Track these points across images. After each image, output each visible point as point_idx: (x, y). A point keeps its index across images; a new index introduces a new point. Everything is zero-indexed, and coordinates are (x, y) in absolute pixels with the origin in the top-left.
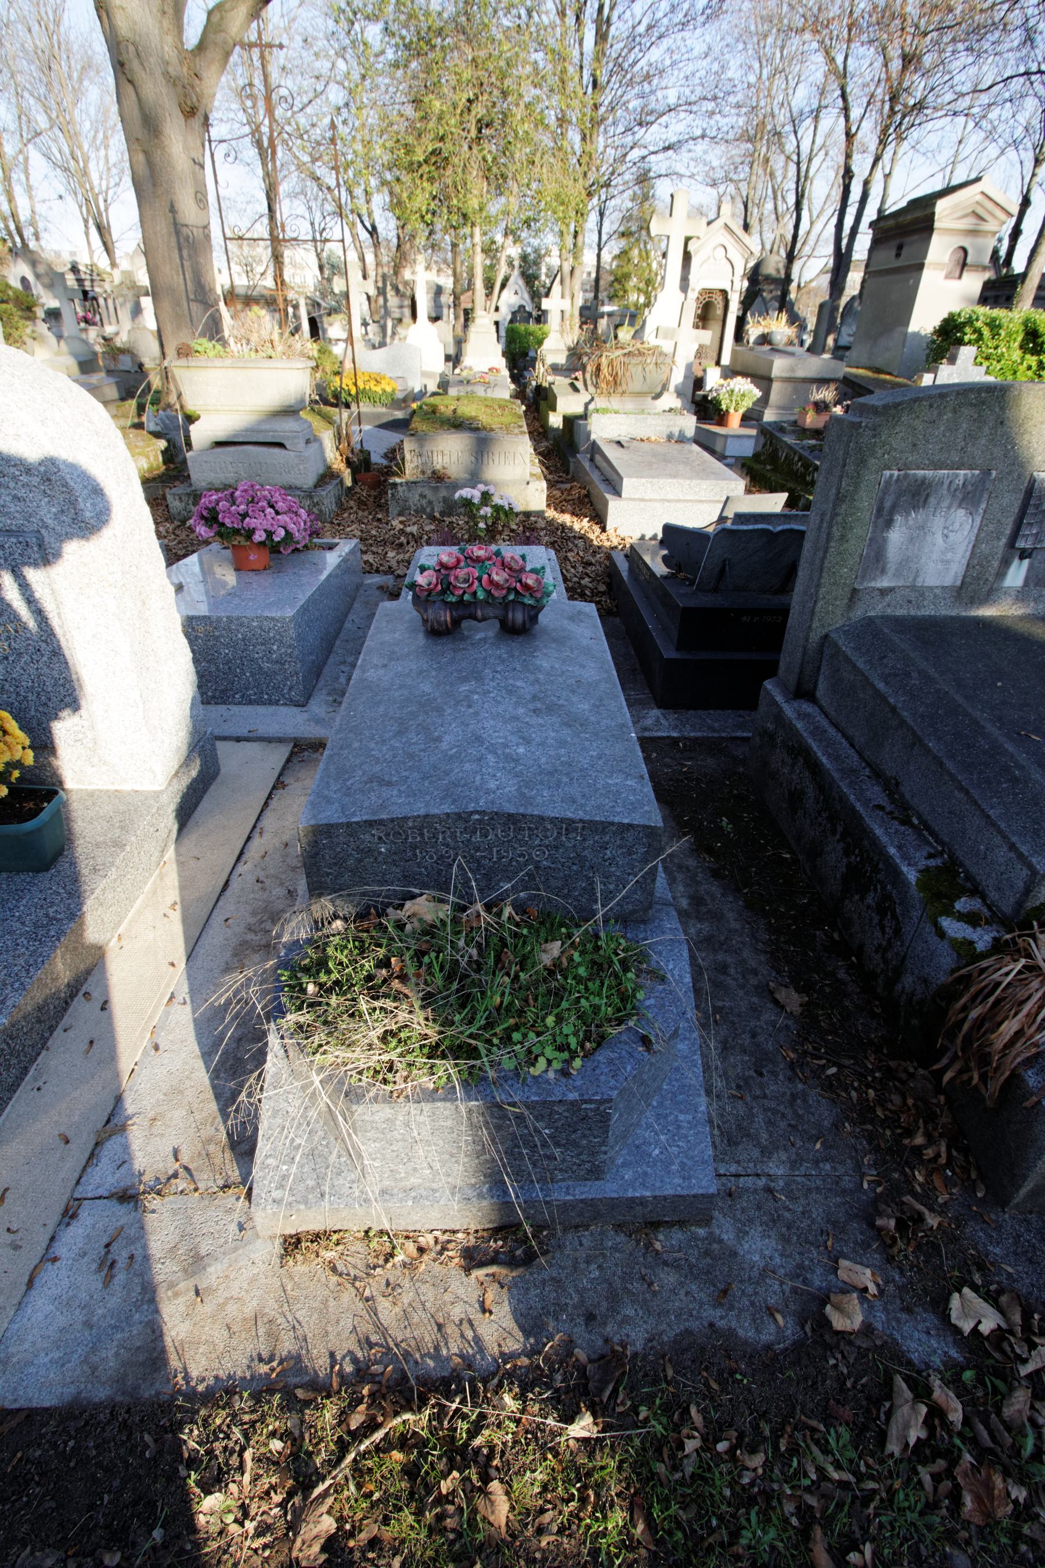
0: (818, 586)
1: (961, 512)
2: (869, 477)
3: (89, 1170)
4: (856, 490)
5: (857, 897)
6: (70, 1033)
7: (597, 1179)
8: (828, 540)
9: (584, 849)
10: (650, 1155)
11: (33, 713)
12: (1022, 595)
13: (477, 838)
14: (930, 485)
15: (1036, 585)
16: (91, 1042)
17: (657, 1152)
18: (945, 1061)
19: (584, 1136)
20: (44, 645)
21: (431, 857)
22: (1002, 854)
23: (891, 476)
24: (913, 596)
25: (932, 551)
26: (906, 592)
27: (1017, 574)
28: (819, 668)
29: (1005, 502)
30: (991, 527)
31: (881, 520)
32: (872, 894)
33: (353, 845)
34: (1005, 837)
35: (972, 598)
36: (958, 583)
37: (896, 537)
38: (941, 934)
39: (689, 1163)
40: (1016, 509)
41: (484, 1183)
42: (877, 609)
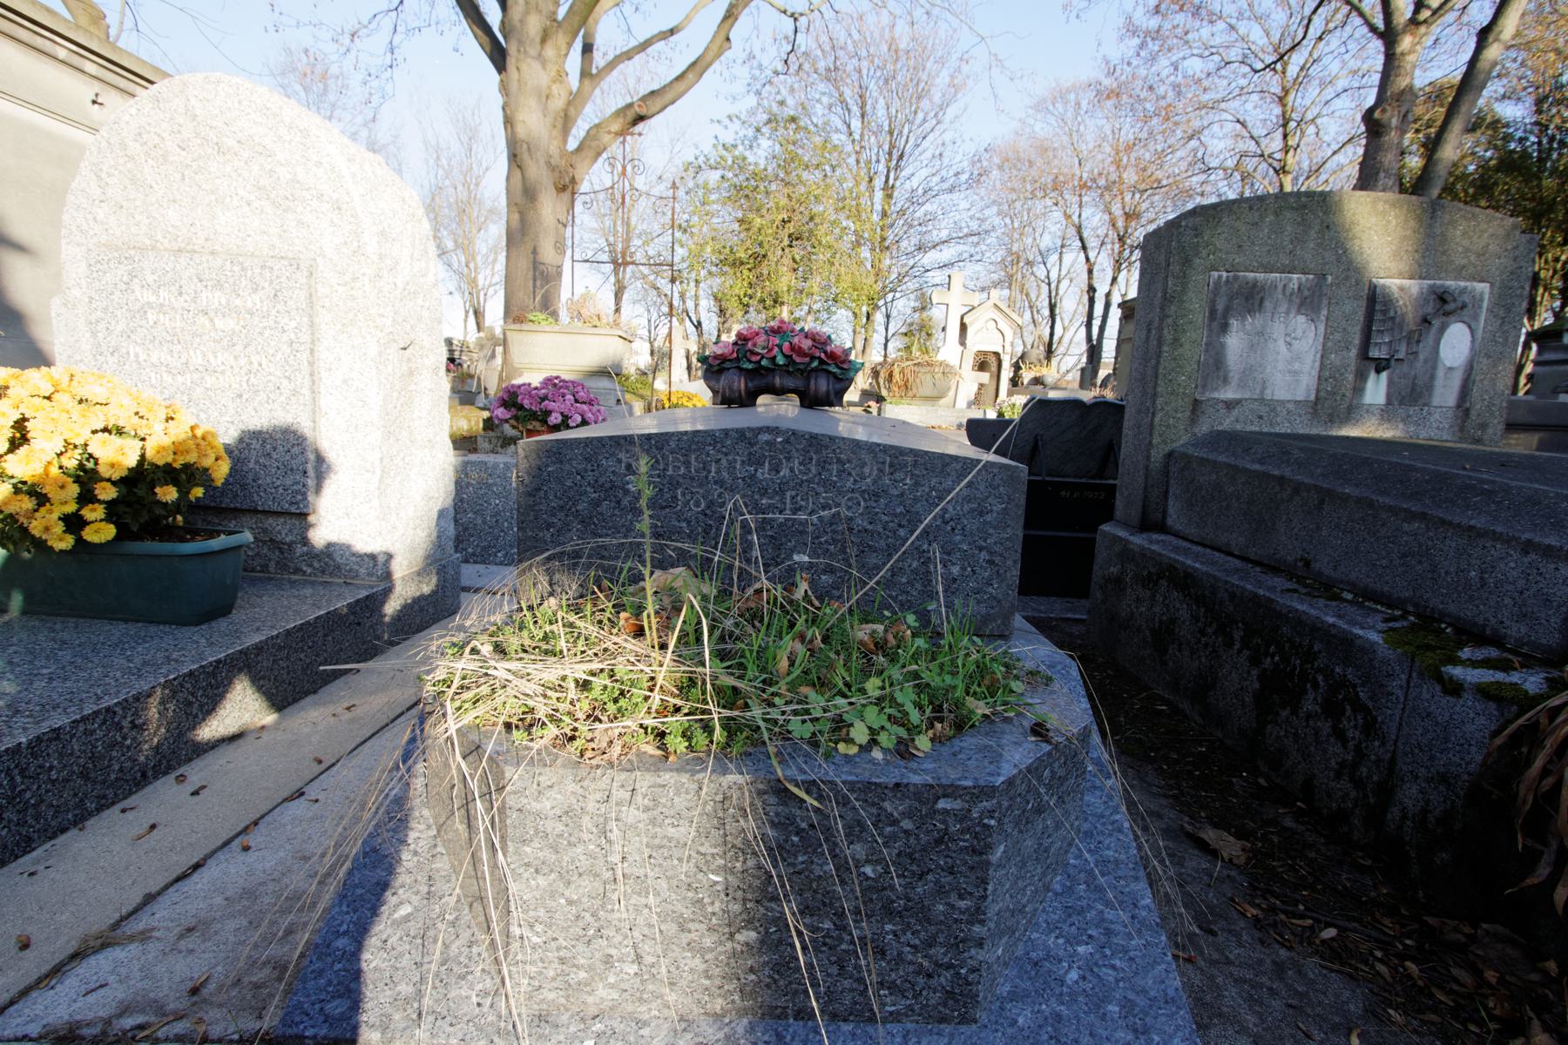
0: (1155, 395)
1: (1301, 319)
2: (1196, 278)
3: (34, 994)
4: (1184, 291)
5: (1285, 713)
6: (130, 815)
7: (965, 1020)
8: (1160, 345)
9: (916, 500)
10: (1062, 982)
11: (251, 465)
12: (1387, 412)
13: (764, 473)
14: (1263, 288)
15: (1401, 403)
16: (153, 827)
17: (1073, 975)
18: (1543, 871)
19: (940, 891)
20: (285, 382)
21: (697, 504)
22: (1512, 566)
23: (1220, 277)
24: (1264, 411)
25: (1276, 360)
26: (1255, 406)
27: (1376, 390)
28: (1167, 492)
29: (1348, 308)
30: (1338, 336)
31: (1215, 324)
32: (1311, 696)
33: (590, 477)
34: (1509, 541)
35: (1331, 415)
36: (1312, 397)
37: (1234, 342)
38: (1454, 688)
39: (1141, 1001)
40: (1360, 316)
41: (741, 1013)
42: (1227, 423)
